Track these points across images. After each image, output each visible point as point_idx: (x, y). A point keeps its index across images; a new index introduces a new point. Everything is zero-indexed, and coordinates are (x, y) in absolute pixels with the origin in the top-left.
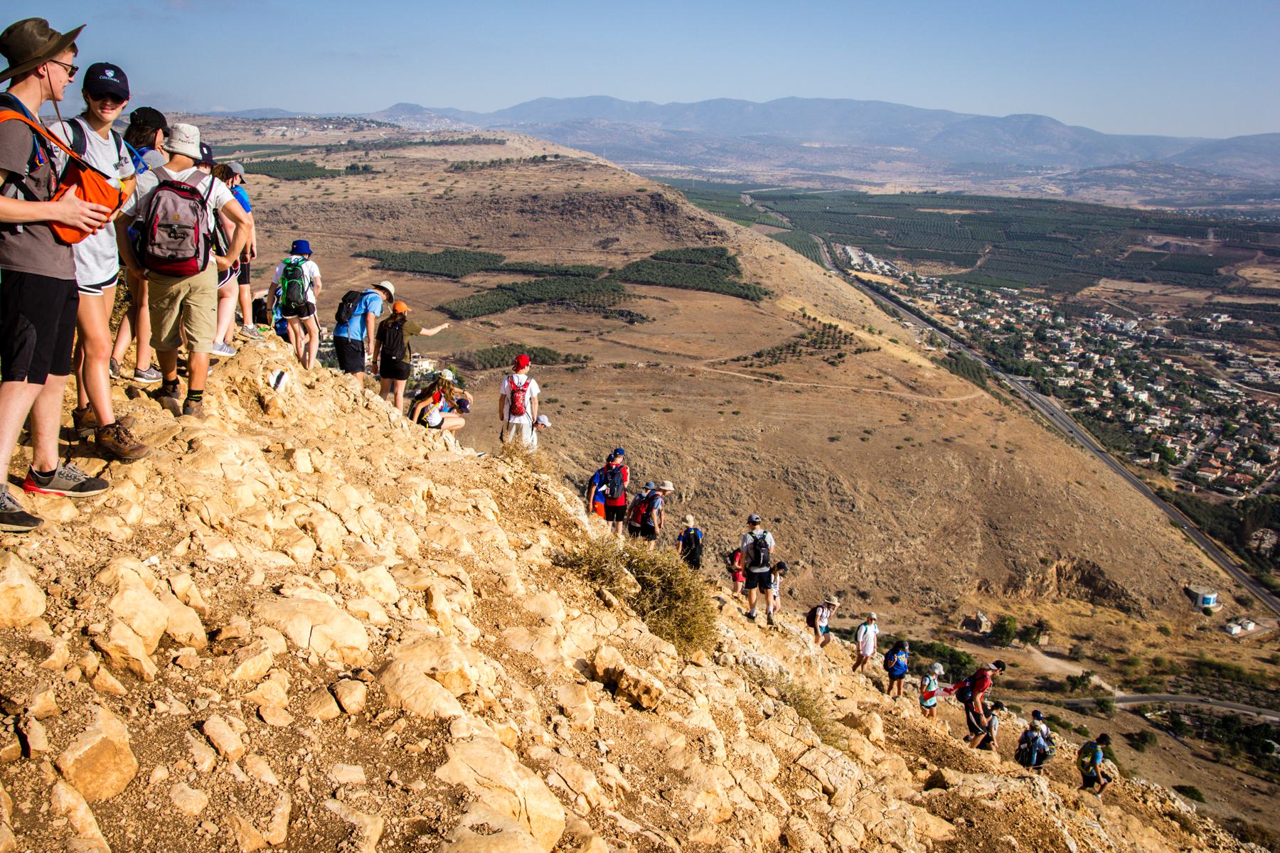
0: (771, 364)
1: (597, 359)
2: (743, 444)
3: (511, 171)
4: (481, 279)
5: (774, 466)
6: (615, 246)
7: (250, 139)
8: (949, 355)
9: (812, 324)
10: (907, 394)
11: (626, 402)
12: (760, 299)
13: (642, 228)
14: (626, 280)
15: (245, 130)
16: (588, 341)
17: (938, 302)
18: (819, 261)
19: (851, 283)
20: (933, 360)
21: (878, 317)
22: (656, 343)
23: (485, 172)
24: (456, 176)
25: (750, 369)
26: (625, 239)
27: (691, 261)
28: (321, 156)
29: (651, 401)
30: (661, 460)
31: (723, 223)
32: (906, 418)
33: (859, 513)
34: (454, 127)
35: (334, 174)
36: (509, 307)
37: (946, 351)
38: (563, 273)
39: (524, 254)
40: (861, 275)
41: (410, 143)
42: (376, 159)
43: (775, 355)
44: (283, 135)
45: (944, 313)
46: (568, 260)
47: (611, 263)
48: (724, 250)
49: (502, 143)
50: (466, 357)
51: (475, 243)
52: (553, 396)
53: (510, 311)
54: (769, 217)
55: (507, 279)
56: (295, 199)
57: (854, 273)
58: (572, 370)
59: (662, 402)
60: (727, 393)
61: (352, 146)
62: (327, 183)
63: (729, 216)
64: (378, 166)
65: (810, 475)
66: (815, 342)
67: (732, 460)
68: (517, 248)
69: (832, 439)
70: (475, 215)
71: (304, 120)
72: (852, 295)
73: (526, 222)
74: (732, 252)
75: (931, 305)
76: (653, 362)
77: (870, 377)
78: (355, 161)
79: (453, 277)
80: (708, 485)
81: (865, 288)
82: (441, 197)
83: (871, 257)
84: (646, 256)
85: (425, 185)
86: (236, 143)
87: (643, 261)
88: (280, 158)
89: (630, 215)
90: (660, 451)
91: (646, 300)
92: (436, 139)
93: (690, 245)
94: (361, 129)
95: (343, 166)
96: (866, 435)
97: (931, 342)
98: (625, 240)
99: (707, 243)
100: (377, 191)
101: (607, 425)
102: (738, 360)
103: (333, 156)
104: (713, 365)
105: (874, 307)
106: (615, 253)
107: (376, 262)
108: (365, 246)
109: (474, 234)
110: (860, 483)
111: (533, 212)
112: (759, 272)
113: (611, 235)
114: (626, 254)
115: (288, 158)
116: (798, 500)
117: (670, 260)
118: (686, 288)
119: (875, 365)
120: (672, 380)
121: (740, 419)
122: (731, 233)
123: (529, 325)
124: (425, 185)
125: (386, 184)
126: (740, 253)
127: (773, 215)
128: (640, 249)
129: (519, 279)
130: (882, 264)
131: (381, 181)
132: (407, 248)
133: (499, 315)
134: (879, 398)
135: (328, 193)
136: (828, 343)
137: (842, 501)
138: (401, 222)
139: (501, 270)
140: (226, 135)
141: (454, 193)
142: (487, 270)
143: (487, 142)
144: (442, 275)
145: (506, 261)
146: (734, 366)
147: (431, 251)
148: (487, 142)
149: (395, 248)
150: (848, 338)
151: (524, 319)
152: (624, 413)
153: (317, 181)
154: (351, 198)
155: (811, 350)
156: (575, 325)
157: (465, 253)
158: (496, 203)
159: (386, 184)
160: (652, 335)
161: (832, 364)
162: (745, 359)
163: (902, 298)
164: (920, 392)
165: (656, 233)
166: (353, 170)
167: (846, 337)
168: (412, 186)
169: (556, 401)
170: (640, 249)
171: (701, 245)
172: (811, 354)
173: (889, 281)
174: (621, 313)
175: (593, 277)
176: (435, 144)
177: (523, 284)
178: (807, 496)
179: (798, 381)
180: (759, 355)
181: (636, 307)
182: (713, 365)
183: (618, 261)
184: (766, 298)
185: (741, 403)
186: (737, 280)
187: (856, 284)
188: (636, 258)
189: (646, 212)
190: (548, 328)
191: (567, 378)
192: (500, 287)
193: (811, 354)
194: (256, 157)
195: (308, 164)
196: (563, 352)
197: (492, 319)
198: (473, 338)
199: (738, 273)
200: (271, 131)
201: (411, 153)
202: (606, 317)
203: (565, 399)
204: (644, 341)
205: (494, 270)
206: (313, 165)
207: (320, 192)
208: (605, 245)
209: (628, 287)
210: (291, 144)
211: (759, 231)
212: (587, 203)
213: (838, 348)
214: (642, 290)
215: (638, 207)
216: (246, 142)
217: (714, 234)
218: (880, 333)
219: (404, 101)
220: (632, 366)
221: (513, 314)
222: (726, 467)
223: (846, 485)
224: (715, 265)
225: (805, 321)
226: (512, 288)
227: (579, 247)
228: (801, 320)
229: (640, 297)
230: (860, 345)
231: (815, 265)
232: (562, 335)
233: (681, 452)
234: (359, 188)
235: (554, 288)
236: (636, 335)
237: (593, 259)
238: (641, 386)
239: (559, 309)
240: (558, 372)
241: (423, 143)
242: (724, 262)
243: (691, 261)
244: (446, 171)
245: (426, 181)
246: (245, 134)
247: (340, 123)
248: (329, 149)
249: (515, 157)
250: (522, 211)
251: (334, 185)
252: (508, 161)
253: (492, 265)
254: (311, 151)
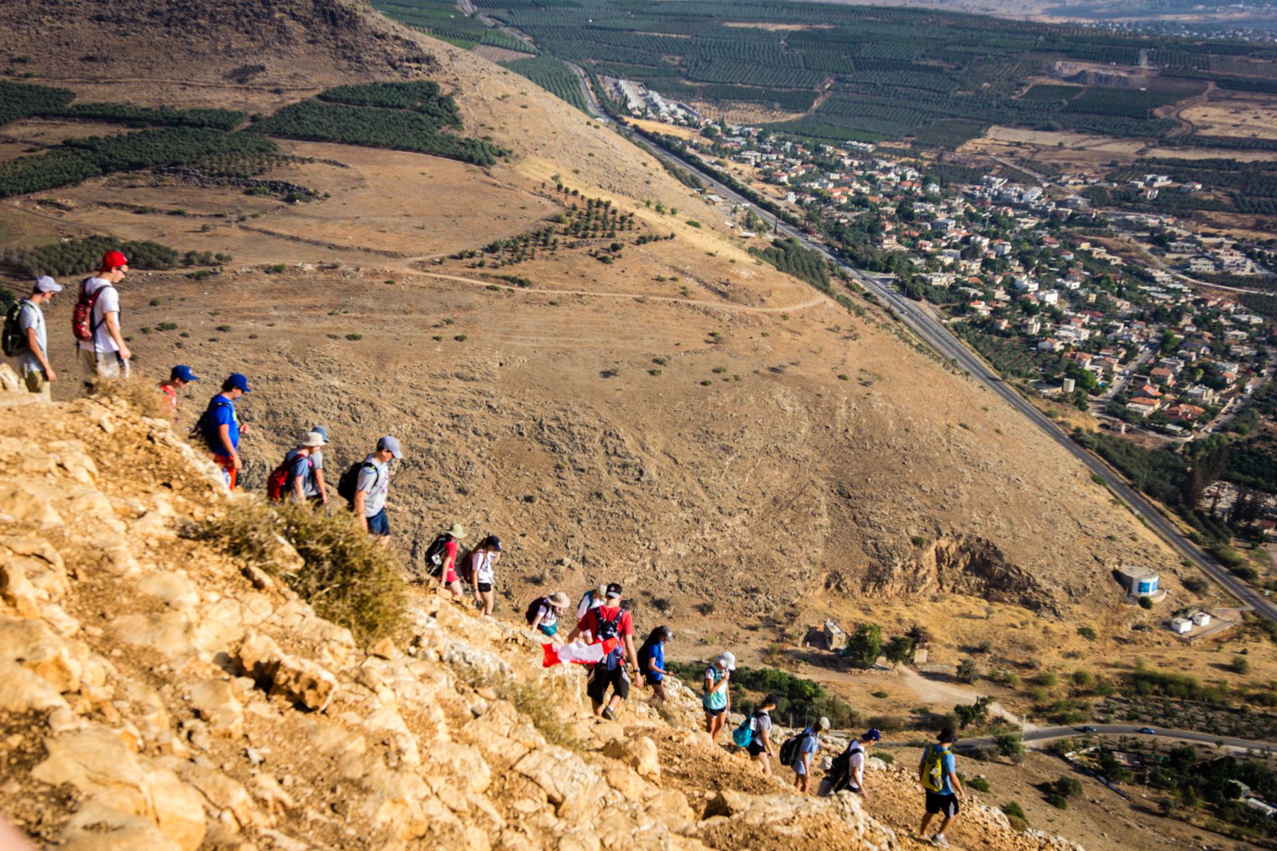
0: (511, 262)
1: (237, 259)
2: (473, 385)
4: (35, 130)
5: (520, 417)
6: (259, 79)
8: (775, 243)
9: (571, 200)
10: (715, 303)
11: (288, 326)
12: (491, 163)
13: (301, 49)
14: (280, 134)
16: (222, 230)
17: (757, 165)
18: (579, 104)
19: (628, 137)
20: (751, 251)
21: (670, 188)
22: (332, 232)
25: (478, 270)
26: (274, 68)
27: (381, 104)
29: (327, 324)
30: (346, 415)
31: (430, 44)
32: (715, 339)
33: (650, 483)
36: (86, 176)
37: (770, 237)
38: (174, 122)
39: (107, 89)
40: (643, 124)
43: (517, 248)
45: (766, 181)
46: (183, 100)
47: (254, 106)
48: (433, 86)
50: (15, 258)
51: (20, 69)
52: (168, 319)
53: (89, 184)
54: (501, 35)
55: (80, 131)
57: (632, 121)
58: (198, 277)
59: (344, 324)
60: (446, 308)
63: (438, 32)
65: (575, 430)
66: (576, 227)
67: (456, 410)
68: (95, 80)
69: (606, 374)
72: (631, 156)
73: (108, 37)
74: (445, 90)
75: (747, 169)
76: (328, 261)
77: (659, 279)
80: (421, 451)
81: (650, 145)
83: (657, 97)
84: (310, 95)
87: (306, 103)
89: (282, 30)
90: (345, 400)
91: (312, 164)
93: (380, 78)
96: (657, 367)
97: (748, 224)
98: (274, 68)
99: (405, 74)
101: (259, 362)
102: (461, 257)
104: (422, 265)
105: (663, 174)
106: (260, 90)
109: (17, 55)
110: (649, 438)
111: (119, 21)
112: (489, 121)
113: (252, 61)
114: (278, 92)
116: (558, 467)
117: (348, 101)
118: (375, 145)
119: (667, 260)
120: (359, 290)
121: (466, 347)
122: (443, 59)
123: (121, 206)
126: (457, 90)
127: (507, 30)
128: (300, 83)
129: (101, 131)
130: (673, 107)
133: (70, 190)
134: (674, 310)
136: (595, 229)
137: (625, 466)
139: (68, 116)
142: (44, 116)
145: (77, 101)
146: (455, 266)
150: (626, 221)
151: (111, 195)
152: (285, 344)
155: (570, 239)
156: (199, 205)
160: (324, 220)
161: (604, 260)
162: (472, 255)
163: (705, 160)
164: (734, 300)
165: (326, 58)
167: (623, 219)
169: (173, 327)
170: (300, 83)
171: (396, 77)
172: (572, 246)
173: (684, 134)
174: (274, 187)
175: (226, 128)
177: (108, 138)
178: (573, 461)
179: (553, 288)
180: (492, 249)
181: (299, 175)
182: (422, 265)
183: (264, 104)
184: (500, 161)
185: (468, 322)
186: (455, 132)
187: (636, 138)
188: (294, 98)
189: (307, 24)
190: (153, 211)
191: (190, 290)
192: (68, 144)
193: (572, 246)
196: (182, 248)
197: (59, 196)
198: (27, 226)
199: (456, 122)
202: (249, 193)
203: (187, 323)
204: (312, 230)
205: (56, 115)
208: (242, 76)
209: (283, 145)
211: (488, 57)
212: (209, 8)
213: (611, 236)
214: (306, 149)
215: (294, 16)
217: (417, 60)
218: (673, 212)
220: (294, 270)
221: (93, 187)
222: (448, 422)
223: (629, 443)
224: (420, 110)
225: (561, 196)
226: (90, 145)
227: (199, 79)
228: (555, 194)
229: (303, 161)
230: (644, 232)
231: (573, 109)
232: (178, 222)
233: (378, 402)
235: (161, 146)
236: (298, 220)
237: (224, 99)
238: (310, 301)
239: (170, 179)
240: (174, 280)
242: (433, 105)
243: (381, 104)
250: (100, 18)
253: (52, 106)
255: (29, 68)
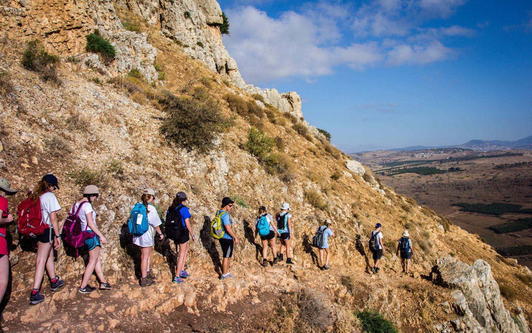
3: (525, 168)
4: (510, 216)
7: (409, 159)
15: (407, 155)
23: (512, 169)
24: (498, 171)
28: (438, 164)
34: (498, 148)
35: (443, 172)
36: (524, 228)
41: (477, 157)
42: (462, 165)
44: (423, 156)
49: (521, 155)
50: (502, 250)
51: (507, 200)
53: (524, 231)
55: (523, 216)
56: (427, 182)
61: (451, 159)
62: (441, 176)
64: (463, 167)
68: (529, 202)
70: (507, 187)
71: (431, 150)
78: (453, 166)
79: (497, 215)
82: (491, 180)
85: (484, 175)
86: (404, 160)
88: (421, 166)
92: (489, 154)
94: (455, 152)
95: (447, 168)
100: (462, 178)
103: (443, 164)
107: (461, 208)
108: (456, 201)
109: (507, 196)
115: (424, 165)
124: (484, 175)
125: (466, 175)
131: (464, 174)
132: (475, 202)
133: (519, 232)
135: (441, 179)
138: (473, 191)
139: (520, 212)
140: (400, 158)
141: (497, 178)
142: (513, 212)
143: (513, 155)
144: (491, 214)
145: (523, 208)
147: (487, 203)
148: (513, 155)
149: (470, 202)
153: (437, 175)
154: (451, 181)
157: (503, 204)
158: (518, 182)
159: (466, 175)
166: (452, 170)
168: (478, 176)
176: (488, 157)
194: (412, 166)
195: (433, 168)
197: (516, 234)
200: (418, 155)
201: (478, 162)
205: (517, 212)
206: (435, 168)
207: (438, 179)
210: (426, 160)
216: (408, 160)
219: (475, 139)
221: (526, 231)
226: (526, 220)
234: (454, 177)
241: (483, 157)
244: (493, 169)
245: (484, 173)
246: (407, 157)
247: (446, 150)
248: (441, 161)
249: (527, 161)
251: (444, 176)
252: (524, 163)
253: (516, 209)
254: (434, 162)
255: (510, 199)
